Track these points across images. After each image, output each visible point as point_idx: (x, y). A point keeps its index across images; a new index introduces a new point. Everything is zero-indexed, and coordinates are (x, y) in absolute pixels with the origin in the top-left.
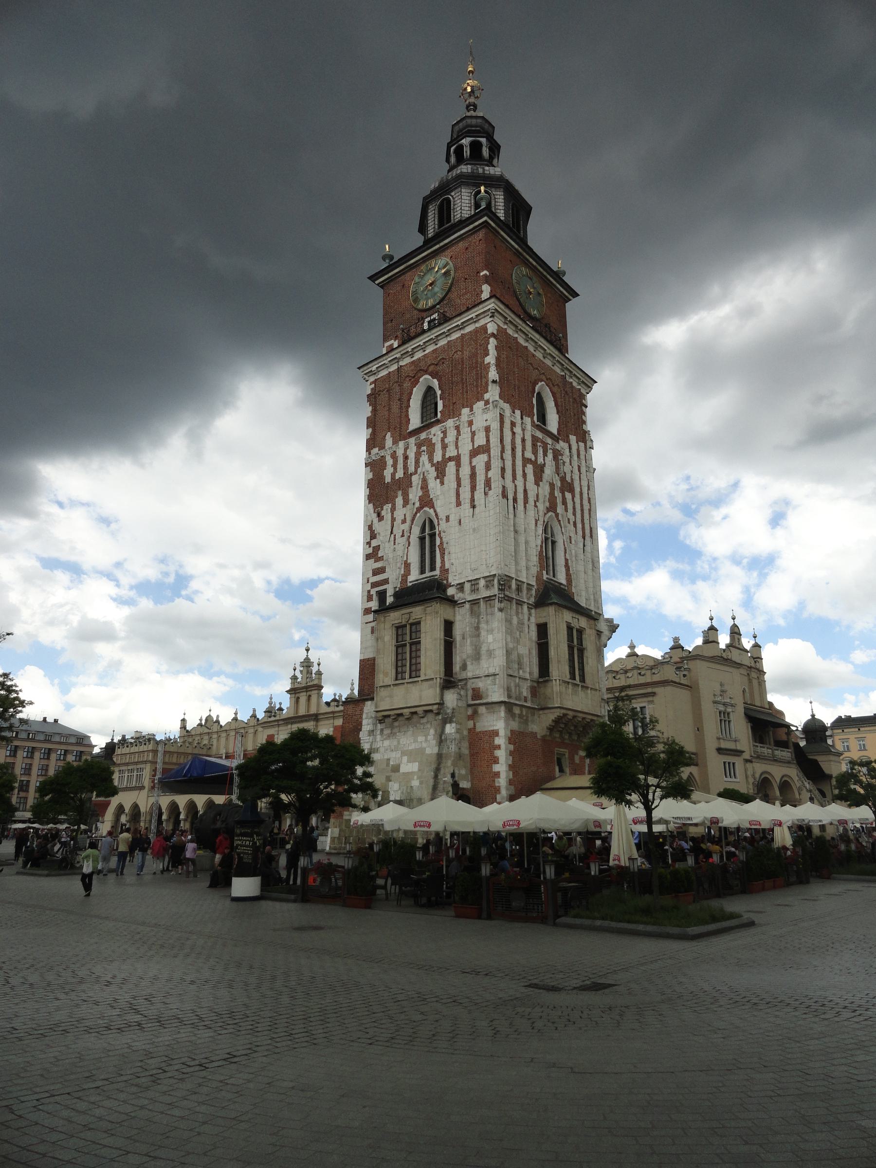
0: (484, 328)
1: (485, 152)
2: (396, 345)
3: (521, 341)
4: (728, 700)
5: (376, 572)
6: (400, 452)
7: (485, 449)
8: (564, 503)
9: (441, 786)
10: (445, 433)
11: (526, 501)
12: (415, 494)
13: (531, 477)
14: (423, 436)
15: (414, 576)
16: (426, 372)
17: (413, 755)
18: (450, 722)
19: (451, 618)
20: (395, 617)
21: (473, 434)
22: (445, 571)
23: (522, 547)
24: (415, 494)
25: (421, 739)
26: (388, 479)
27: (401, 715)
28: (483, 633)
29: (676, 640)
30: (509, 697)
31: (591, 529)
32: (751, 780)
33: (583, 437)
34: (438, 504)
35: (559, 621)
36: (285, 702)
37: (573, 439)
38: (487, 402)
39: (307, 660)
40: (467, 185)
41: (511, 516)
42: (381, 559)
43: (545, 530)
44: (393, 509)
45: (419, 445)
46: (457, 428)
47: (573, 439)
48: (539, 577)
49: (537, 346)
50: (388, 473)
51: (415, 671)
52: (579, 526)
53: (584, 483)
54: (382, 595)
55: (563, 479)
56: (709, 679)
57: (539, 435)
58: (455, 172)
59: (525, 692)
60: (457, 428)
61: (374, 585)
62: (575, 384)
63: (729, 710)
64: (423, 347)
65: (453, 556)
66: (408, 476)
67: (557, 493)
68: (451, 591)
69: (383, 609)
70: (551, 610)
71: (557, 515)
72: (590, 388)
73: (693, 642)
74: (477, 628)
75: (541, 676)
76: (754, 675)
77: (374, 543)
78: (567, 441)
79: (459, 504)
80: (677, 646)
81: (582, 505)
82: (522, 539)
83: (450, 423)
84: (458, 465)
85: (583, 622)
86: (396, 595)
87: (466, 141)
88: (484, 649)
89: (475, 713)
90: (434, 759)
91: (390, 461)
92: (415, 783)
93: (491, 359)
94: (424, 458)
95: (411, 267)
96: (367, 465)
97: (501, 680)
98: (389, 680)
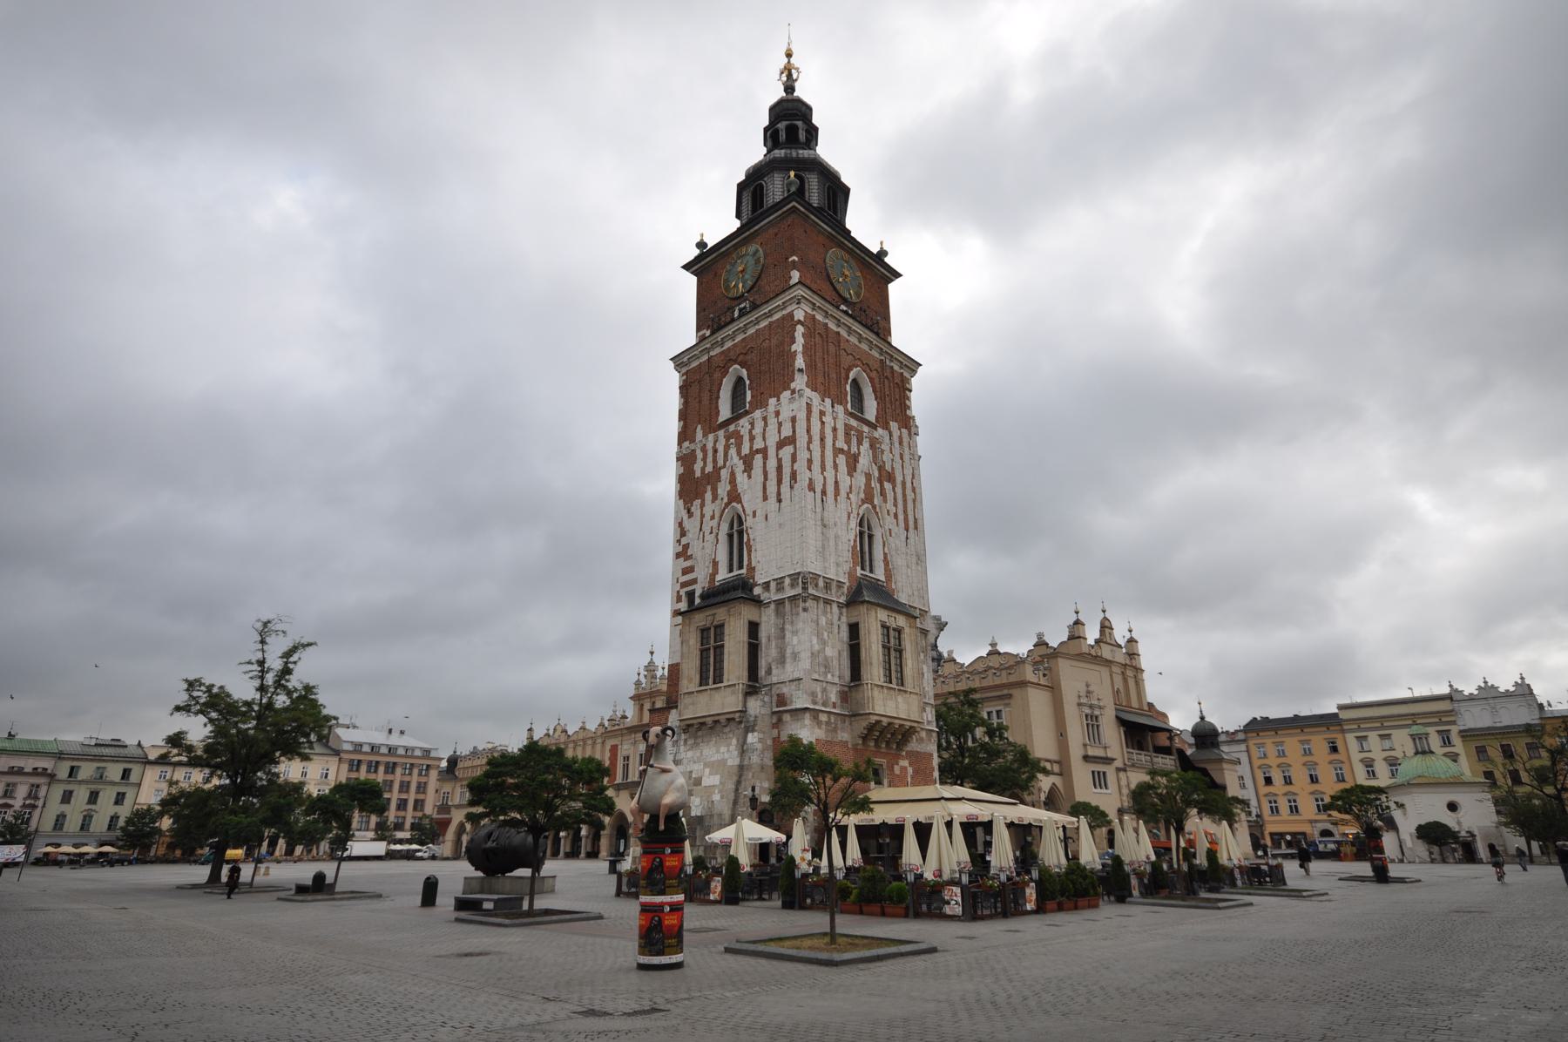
0: (791, 315)
1: (802, 136)
2: (708, 333)
3: (832, 326)
4: (1095, 702)
6: (710, 446)
7: (791, 440)
8: (883, 493)
9: (741, 801)
10: (752, 424)
11: (837, 493)
12: (723, 489)
13: (843, 467)
14: (732, 428)
15: (723, 574)
16: (735, 362)
17: (716, 767)
18: (753, 731)
19: (755, 618)
20: (700, 619)
21: (780, 424)
22: (752, 569)
23: (832, 543)
24: (723, 489)
25: (723, 749)
26: (698, 474)
27: (703, 724)
28: (788, 635)
29: (1040, 636)
30: (815, 703)
31: (916, 520)
32: (1125, 791)
33: (907, 422)
34: (745, 499)
35: (873, 622)
36: (630, 711)
37: (894, 425)
38: (793, 392)
39: (651, 663)
40: (780, 169)
41: (819, 510)
42: (690, 557)
43: (861, 524)
44: (702, 505)
45: (727, 438)
46: (765, 419)
47: (894, 425)
48: (851, 574)
49: (850, 331)
50: (698, 467)
51: (719, 678)
52: (901, 517)
53: (908, 472)
55: (881, 469)
56: (1073, 679)
57: (854, 423)
58: (771, 156)
59: (833, 698)
60: (765, 419)
61: (684, 585)
62: (896, 368)
63: (1097, 712)
64: (733, 337)
65: (759, 553)
66: (717, 470)
67: (875, 484)
68: (757, 591)
69: (692, 609)
70: (863, 609)
71: (874, 507)
72: (914, 372)
73: (1056, 638)
74: (783, 630)
75: (853, 680)
76: (1130, 673)
77: (684, 541)
78: (886, 427)
79: (765, 498)
80: (1041, 643)
81: (904, 495)
82: (831, 533)
83: (758, 414)
84: (765, 458)
85: (901, 621)
86: (702, 597)
87: (782, 126)
88: (789, 651)
89: (780, 720)
90: (735, 770)
91: (700, 455)
92: (716, 797)
93: (798, 346)
94: (733, 451)
96: (678, 459)
98: (694, 687)
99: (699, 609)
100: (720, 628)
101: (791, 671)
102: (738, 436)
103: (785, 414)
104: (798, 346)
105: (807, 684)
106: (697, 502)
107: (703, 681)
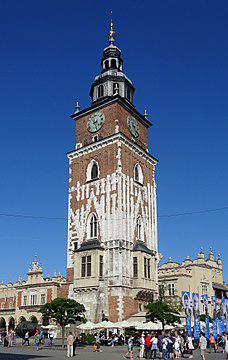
0: (116, 144)
1: (117, 64)
5: (73, 235)
12: (89, 207)
14: (92, 184)
15: (88, 237)
20: (82, 254)
24: (89, 207)
35: (141, 256)
50: (78, 197)
54: (76, 244)
57: (136, 185)
68: (102, 245)
83: (102, 180)
93: (118, 156)
95: (89, 113)
97: (121, 278)
99: (79, 251)
100: (89, 257)
101: (115, 273)
102: (94, 187)
103: (114, 182)
104: (118, 156)
105: (121, 278)
106: (78, 211)
107: (83, 275)
